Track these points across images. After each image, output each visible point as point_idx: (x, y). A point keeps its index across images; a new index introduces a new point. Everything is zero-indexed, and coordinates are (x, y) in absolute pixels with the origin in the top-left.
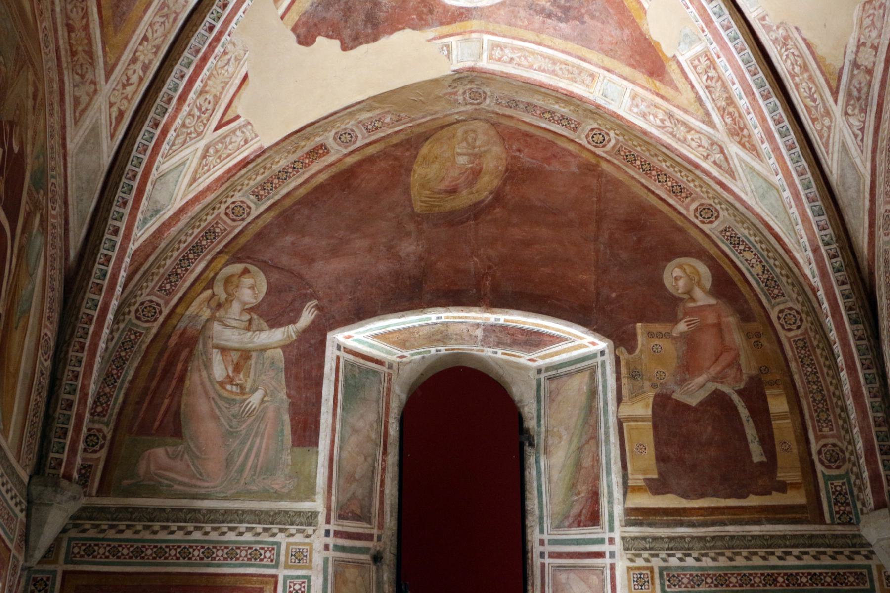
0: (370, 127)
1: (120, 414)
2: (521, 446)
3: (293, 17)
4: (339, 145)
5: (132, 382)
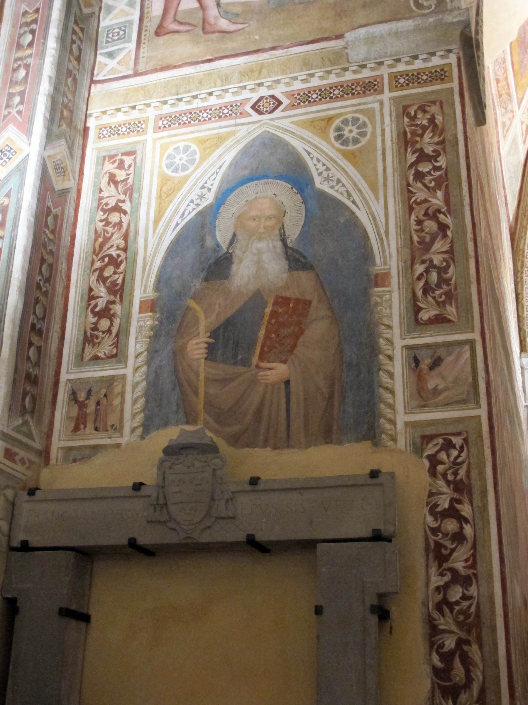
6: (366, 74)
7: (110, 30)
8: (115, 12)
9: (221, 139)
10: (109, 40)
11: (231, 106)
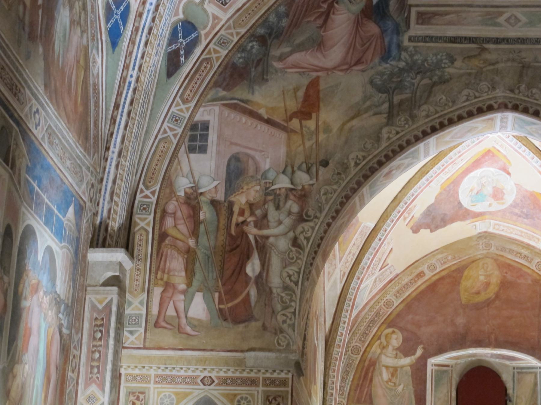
0: (442, 262)
1: (349, 395)
2: (506, 401)
3: (412, 224)
4: (429, 271)
5: (352, 381)
6: (253, 375)
7: (130, 316)
8: (133, 306)
9: (186, 395)
10: (130, 323)
11: (191, 378)
